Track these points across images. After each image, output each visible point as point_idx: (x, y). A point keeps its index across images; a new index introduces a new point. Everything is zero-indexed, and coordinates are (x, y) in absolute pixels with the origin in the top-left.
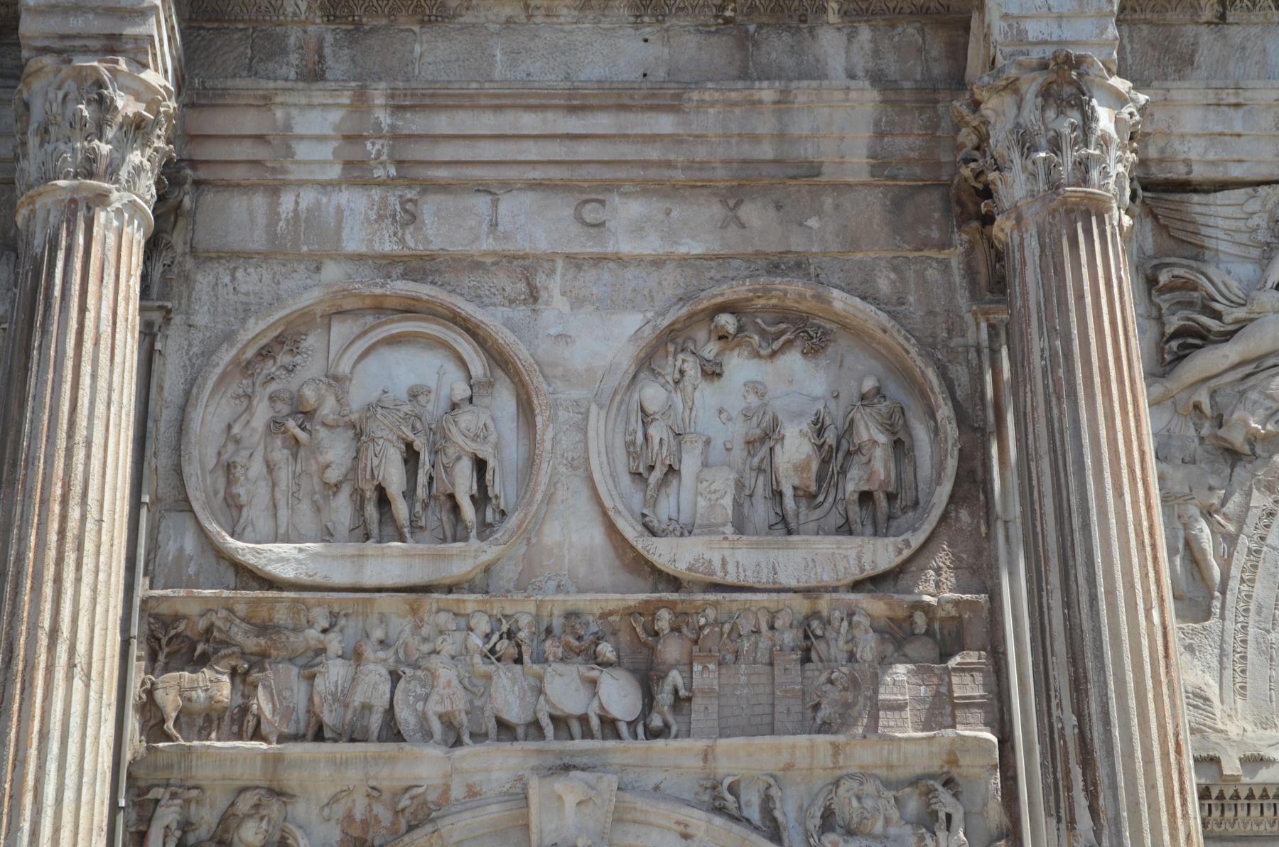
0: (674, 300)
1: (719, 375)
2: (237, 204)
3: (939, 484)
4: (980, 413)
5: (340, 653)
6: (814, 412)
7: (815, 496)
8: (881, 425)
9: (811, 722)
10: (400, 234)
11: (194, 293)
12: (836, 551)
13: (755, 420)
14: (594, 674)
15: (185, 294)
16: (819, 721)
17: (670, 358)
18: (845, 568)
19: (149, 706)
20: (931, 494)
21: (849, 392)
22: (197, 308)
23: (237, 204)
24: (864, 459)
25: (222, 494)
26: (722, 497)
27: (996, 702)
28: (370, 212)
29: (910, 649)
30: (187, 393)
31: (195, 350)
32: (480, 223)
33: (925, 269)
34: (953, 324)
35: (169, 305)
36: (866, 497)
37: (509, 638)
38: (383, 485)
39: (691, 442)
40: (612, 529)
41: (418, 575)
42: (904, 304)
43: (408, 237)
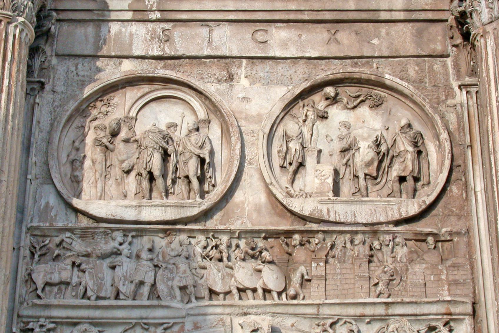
0: (302, 81)
1: (326, 118)
2: (79, 32)
3: (441, 172)
4: (462, 137)
5: (129, 255)
6: (375, 137)
7: (375, 178)
8: (411, 141)
9: (374, 293)
10: (162, 47)
11: (56, 76)
12: (387, 206)
13: (345, 139)
14: (259, 267)
15: (52, 77)
16: (378, 292)
17: (301, 109)
18: (392, 214)
19: (30, 279)
20: (437, 178)
21: (395, 127)
22: (58, 83)
23: (79, 32)
24: (402, 160)
25: (69, 175)
26: (327, 178)
27: (471, 284)
28: (147, 36)
29: (425, 257)
30: (52, 125)
31: (56, 103)
32: (203, 41)
33: (433, 65)
34: (448, 92)
35: (42, 80)
36: (402, 179)
37: (216, 249)
38: (152, 171)
39: (312, 151)
40: (271, 194)
41: (170, 215)
42: (423, 82)
43: (166, 48)
